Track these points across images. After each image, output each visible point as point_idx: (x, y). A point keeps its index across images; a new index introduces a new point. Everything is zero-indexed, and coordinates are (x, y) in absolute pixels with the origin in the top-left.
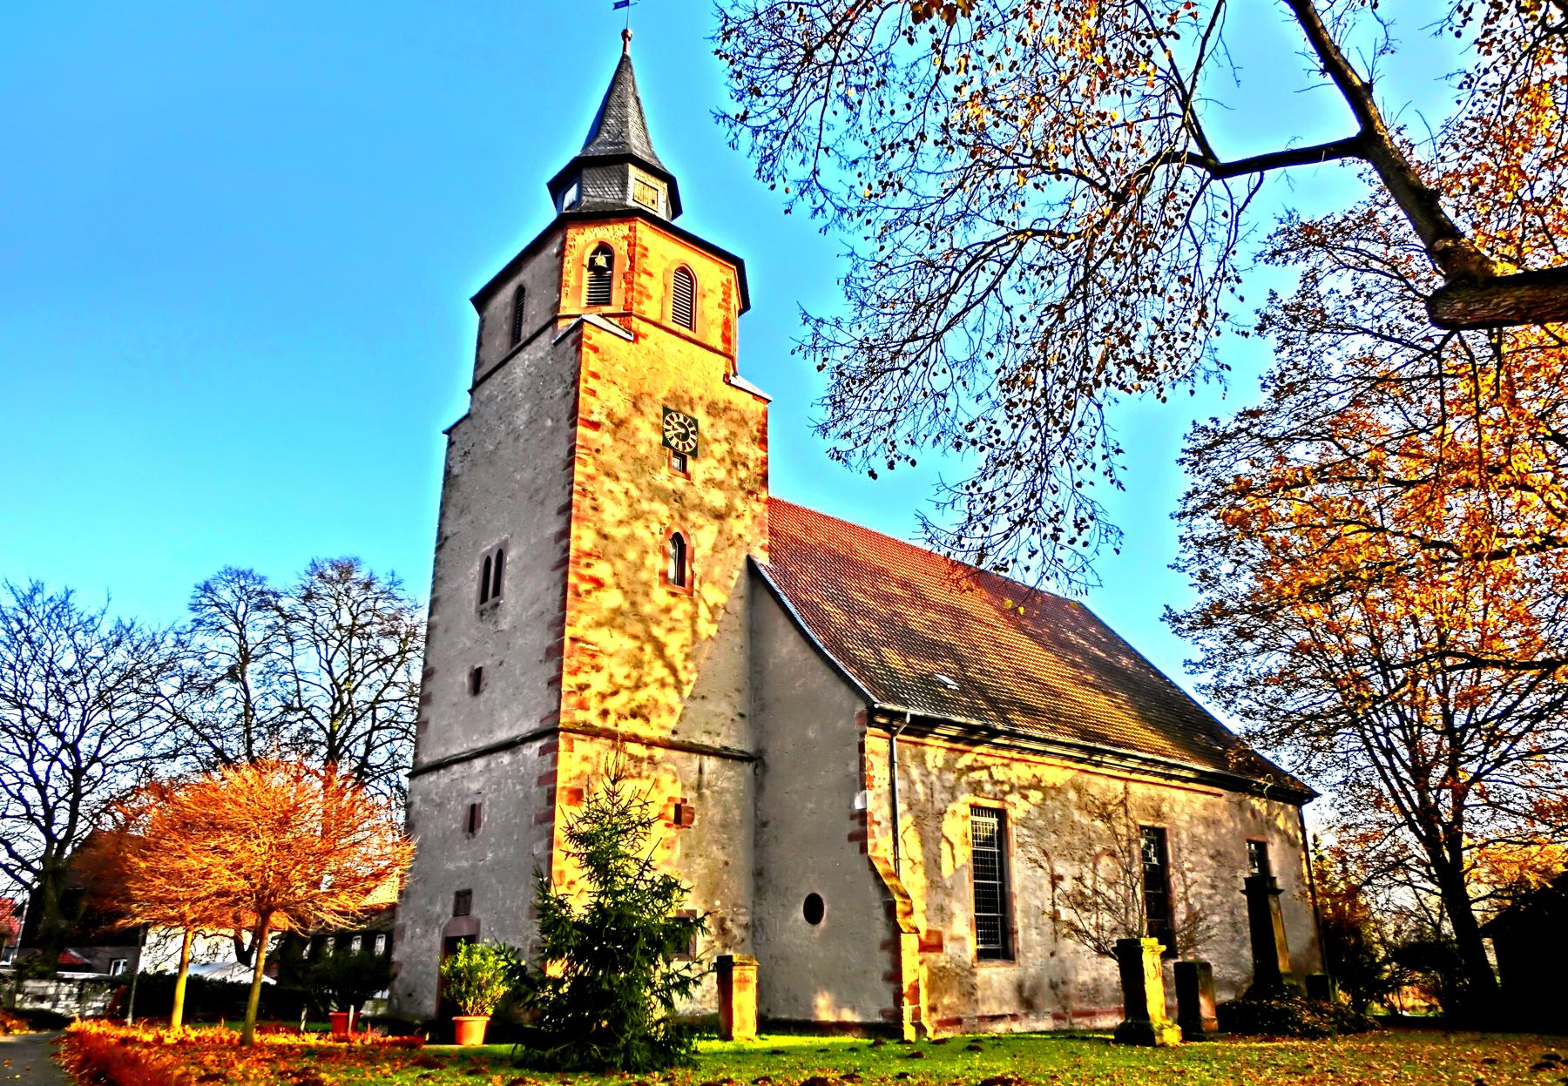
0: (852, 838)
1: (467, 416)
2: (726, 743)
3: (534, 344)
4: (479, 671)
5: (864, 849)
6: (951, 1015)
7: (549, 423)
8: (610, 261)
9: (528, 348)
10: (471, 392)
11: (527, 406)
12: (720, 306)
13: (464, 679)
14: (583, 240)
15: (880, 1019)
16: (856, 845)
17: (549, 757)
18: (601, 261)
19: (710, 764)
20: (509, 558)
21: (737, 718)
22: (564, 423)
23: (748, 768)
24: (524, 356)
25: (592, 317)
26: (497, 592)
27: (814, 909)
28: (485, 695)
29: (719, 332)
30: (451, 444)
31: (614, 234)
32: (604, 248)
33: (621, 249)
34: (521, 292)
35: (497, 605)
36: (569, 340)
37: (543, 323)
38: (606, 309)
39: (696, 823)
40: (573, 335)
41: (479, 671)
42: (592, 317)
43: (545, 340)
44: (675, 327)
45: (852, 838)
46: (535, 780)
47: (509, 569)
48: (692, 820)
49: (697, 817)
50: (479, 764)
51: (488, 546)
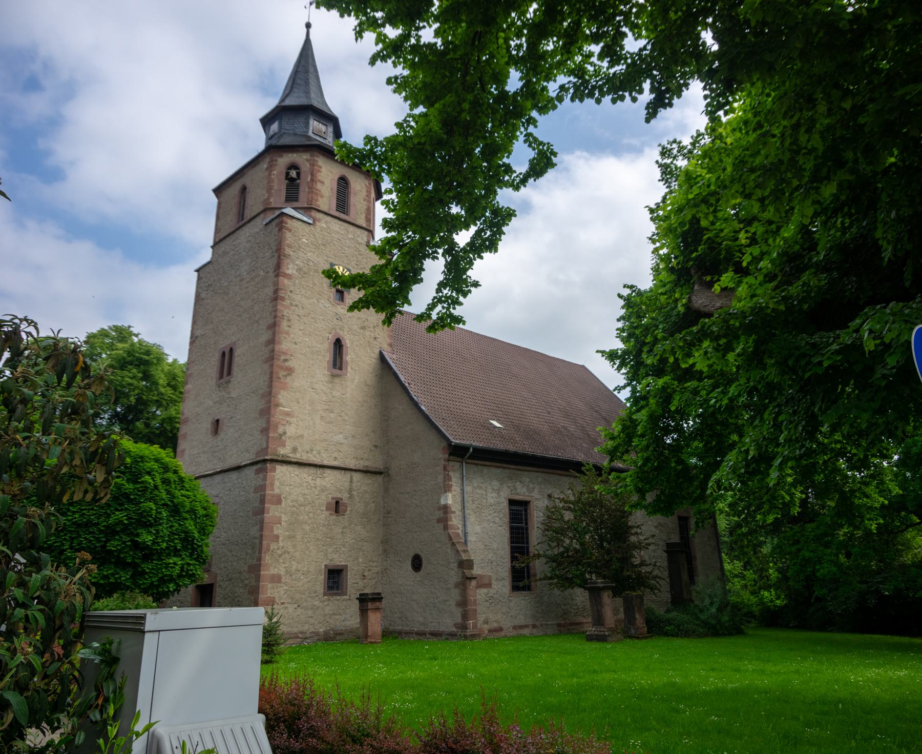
0: (439, 521)
1: (209, 263)
2: (367, 463)
3: (252, 223)
4: (218, 421)
5: (446, 527)
6: (495, 625)
7: (262, 273)
8: (298, 174)
9: (249, 225)
10: (212, 247)
11: (248, 261)
12: (365, 200)
13: (207, 425)
14: (284, 160)
15: (454, 629)
16: (441, 526)
17: (261, 475)
18: (293, 174)
19: (357, 476)
20: (237, 353)
21: (373, 448)
22: (271, 274)
23: (380, 478)
24: (247, 231)
25: (289, 211)
26: (229, 373)
27: (417, 563)
28: (222, 434)
29: (363, 216)
30: (199, 278)
31: (301, 159)
32: (294, 166)
33: (305, 167)
34: (244, 189)
35: (229, 381)
36: (274, 223)
37: (259, 211)
38: (296, 204)
39: (348, 512)
40: (277, 221)
41: (218, 421)
42: (289, 211)
43: (260, 222)
44: (337, 214)
45: (439, 521)
46: (252, 489)
47: (237, 360)
48: (346, 511)
49: (349, 509)
50: (218, 478)
51: (224, 344)
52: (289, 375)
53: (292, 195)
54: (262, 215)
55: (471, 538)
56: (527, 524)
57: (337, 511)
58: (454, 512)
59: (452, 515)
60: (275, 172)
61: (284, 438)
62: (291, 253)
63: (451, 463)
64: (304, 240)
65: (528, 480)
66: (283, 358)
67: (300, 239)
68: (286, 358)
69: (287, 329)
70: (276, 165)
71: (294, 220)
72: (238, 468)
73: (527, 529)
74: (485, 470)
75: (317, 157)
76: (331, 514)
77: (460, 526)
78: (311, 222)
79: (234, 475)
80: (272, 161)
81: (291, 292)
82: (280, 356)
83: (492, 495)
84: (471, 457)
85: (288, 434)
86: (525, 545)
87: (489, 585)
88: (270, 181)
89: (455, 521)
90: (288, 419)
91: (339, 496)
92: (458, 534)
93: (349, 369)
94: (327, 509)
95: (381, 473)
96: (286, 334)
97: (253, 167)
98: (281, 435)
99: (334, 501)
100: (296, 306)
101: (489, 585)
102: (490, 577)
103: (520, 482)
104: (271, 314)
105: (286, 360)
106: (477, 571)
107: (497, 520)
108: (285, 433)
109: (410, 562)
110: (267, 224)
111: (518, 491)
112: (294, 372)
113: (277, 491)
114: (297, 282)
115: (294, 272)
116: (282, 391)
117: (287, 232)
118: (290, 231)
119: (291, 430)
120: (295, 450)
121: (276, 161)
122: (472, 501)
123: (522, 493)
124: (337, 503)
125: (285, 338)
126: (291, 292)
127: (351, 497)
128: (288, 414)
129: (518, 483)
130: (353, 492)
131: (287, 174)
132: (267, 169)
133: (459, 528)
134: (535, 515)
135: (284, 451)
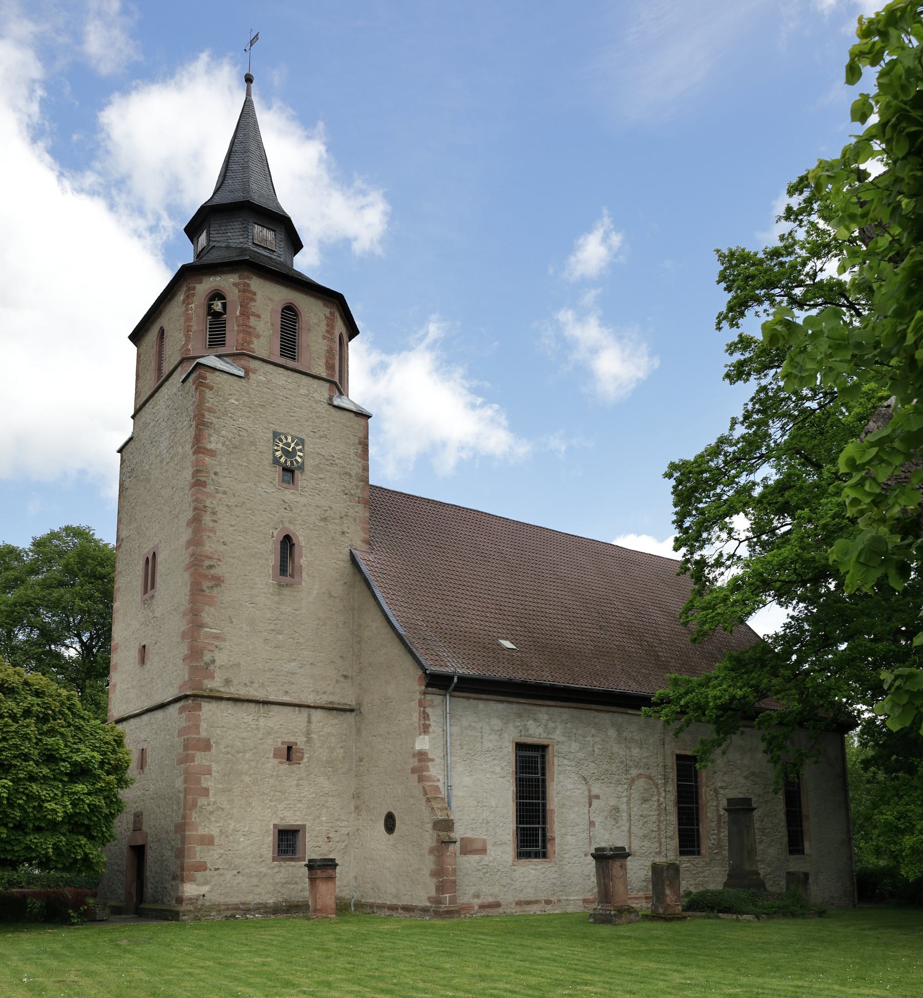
0: (414, 771)
4: (144, 647)
9: (167, 384)
14: (206, 285)
18: (218, 306)
19: (317, 715)
20: (160, 558)
25: (211, 360)
27: (390, 823)
31: (227, 282)
32: (217, 295)
35: (153, 596)
36: (191, 379)
39: (305, 760)
40: (193, 376)
41: (144, 647)
43: (179, 376)
47: (160, 568)
49: (306, 756)
52: (217, 586)
53: (216, 338)
54: (179, 369)
55: (458, 793)
56: (544, 774)
57: (289, 759)
58: (432, 760)
59: (430, 764)
60: (193, 306)
61: (212, 667)
62: (214, 420)
63: (429, 697)
64: (233, 401)
65: (546, 717)
66: (207, 563)
67: (227, 400)
68: (211, 563)
69: (211, 524)
70: (194, 295)
71: (217, 373)
72: (162, 706)
73: (544, 781)
74: (481, 705)
75: (250, 279)
76: (281, 763)
77: (441, 778)
78: (242, 374)
79: (159, 714)
80: (189, 290)
81: (216, 474)
82: (203, 561)
83: (491, 737)
84: (457, 689)
85: (218, 663)
86: (540, 801)
87: (483, 851)
88: (188, 319)
89: (435, 771)
90: (217, 643)
91: (292, 739)
92: (437, 788)
93: (304, 574)
94: (275, 756)
95: (352, 711)
96: (210, 531)
97: (170, 300)
98: (207, 665)
99: (286, 746)
100: (225, 493)
101: (483, 851)
102: (484, 841)
103: (535, 720)
104: (190, 505)
105: (211, 567)
106: (459, 832)
107: (498, 769)
108: (213, 661)
109: (383, 822)
110: (184, 381)
111: (531, 732)
112: (223, 581)
113: (203, 734)
114: (224, 460)
115: (220, 446)
116: (207, 608)
117: (207, 390)
118: (211, 388)
119: (221, 658)
120: (227, 682)
121: (194, 289)
122: (461, 745)
123: (535, 733)
124: (289, 748)
125: (209, 537)
126: (216, 474)
127: (309, 740)
128: (216, 637)
129: (531, 722)
130: (313, 735)
131: (210, 307)
132: (184, 301)
133: (439, 780)
134: (556, 763)
135: (215, 684)
